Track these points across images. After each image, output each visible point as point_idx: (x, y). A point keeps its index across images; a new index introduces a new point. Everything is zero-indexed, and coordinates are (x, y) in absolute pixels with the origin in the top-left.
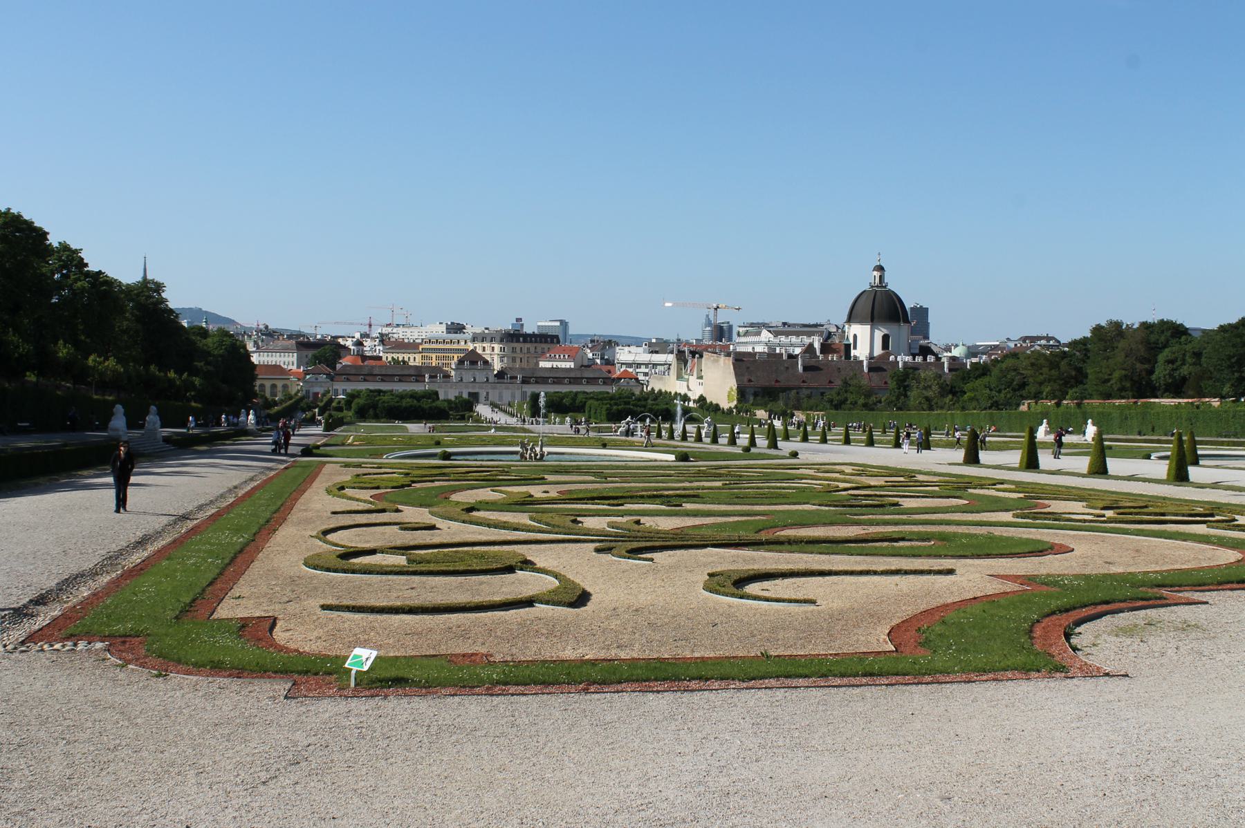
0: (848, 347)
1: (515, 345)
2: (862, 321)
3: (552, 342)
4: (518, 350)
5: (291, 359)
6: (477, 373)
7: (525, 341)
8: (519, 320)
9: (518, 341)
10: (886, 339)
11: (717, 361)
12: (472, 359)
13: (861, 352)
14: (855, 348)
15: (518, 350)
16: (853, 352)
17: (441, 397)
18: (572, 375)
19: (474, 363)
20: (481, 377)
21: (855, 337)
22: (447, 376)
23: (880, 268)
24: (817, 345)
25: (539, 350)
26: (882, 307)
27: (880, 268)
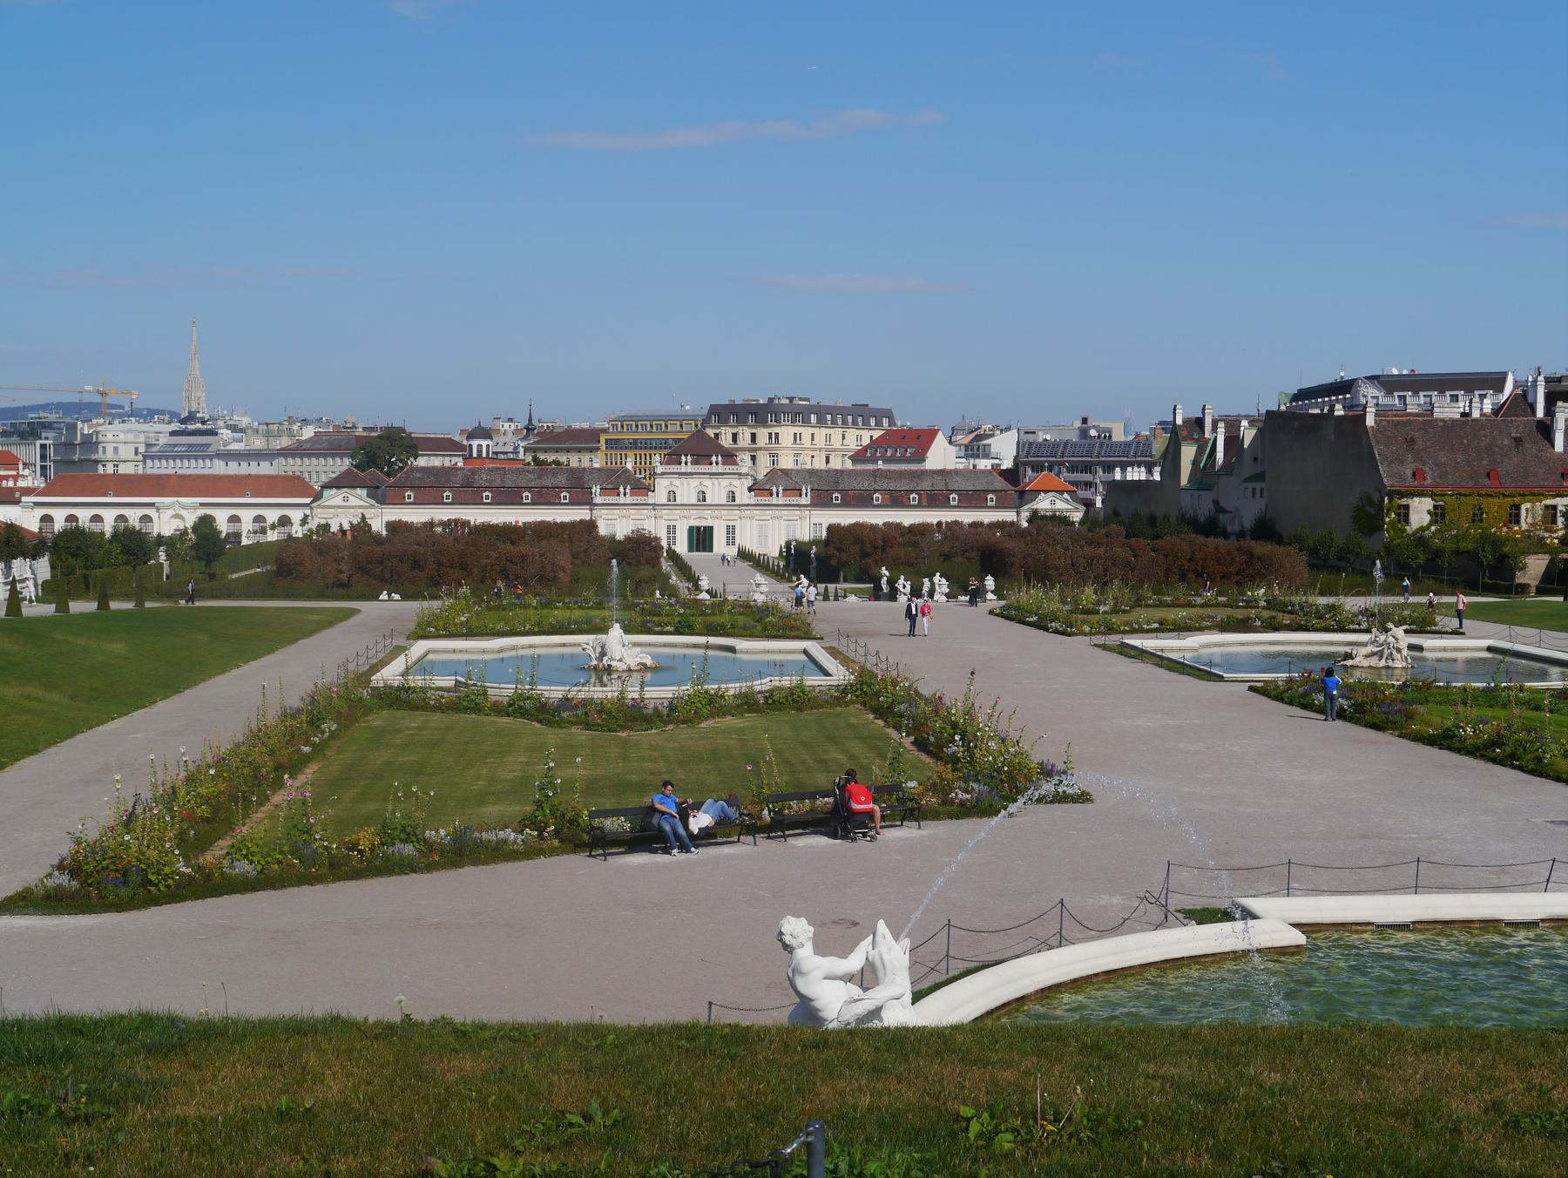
4: (806, 440)
6: (707, 482)
7: (821, 422)
9: (806, 422)
15: (806, 440)
17: (603, 530)
18: (926, 485)
19: (702, 457)
20: (717, 491)
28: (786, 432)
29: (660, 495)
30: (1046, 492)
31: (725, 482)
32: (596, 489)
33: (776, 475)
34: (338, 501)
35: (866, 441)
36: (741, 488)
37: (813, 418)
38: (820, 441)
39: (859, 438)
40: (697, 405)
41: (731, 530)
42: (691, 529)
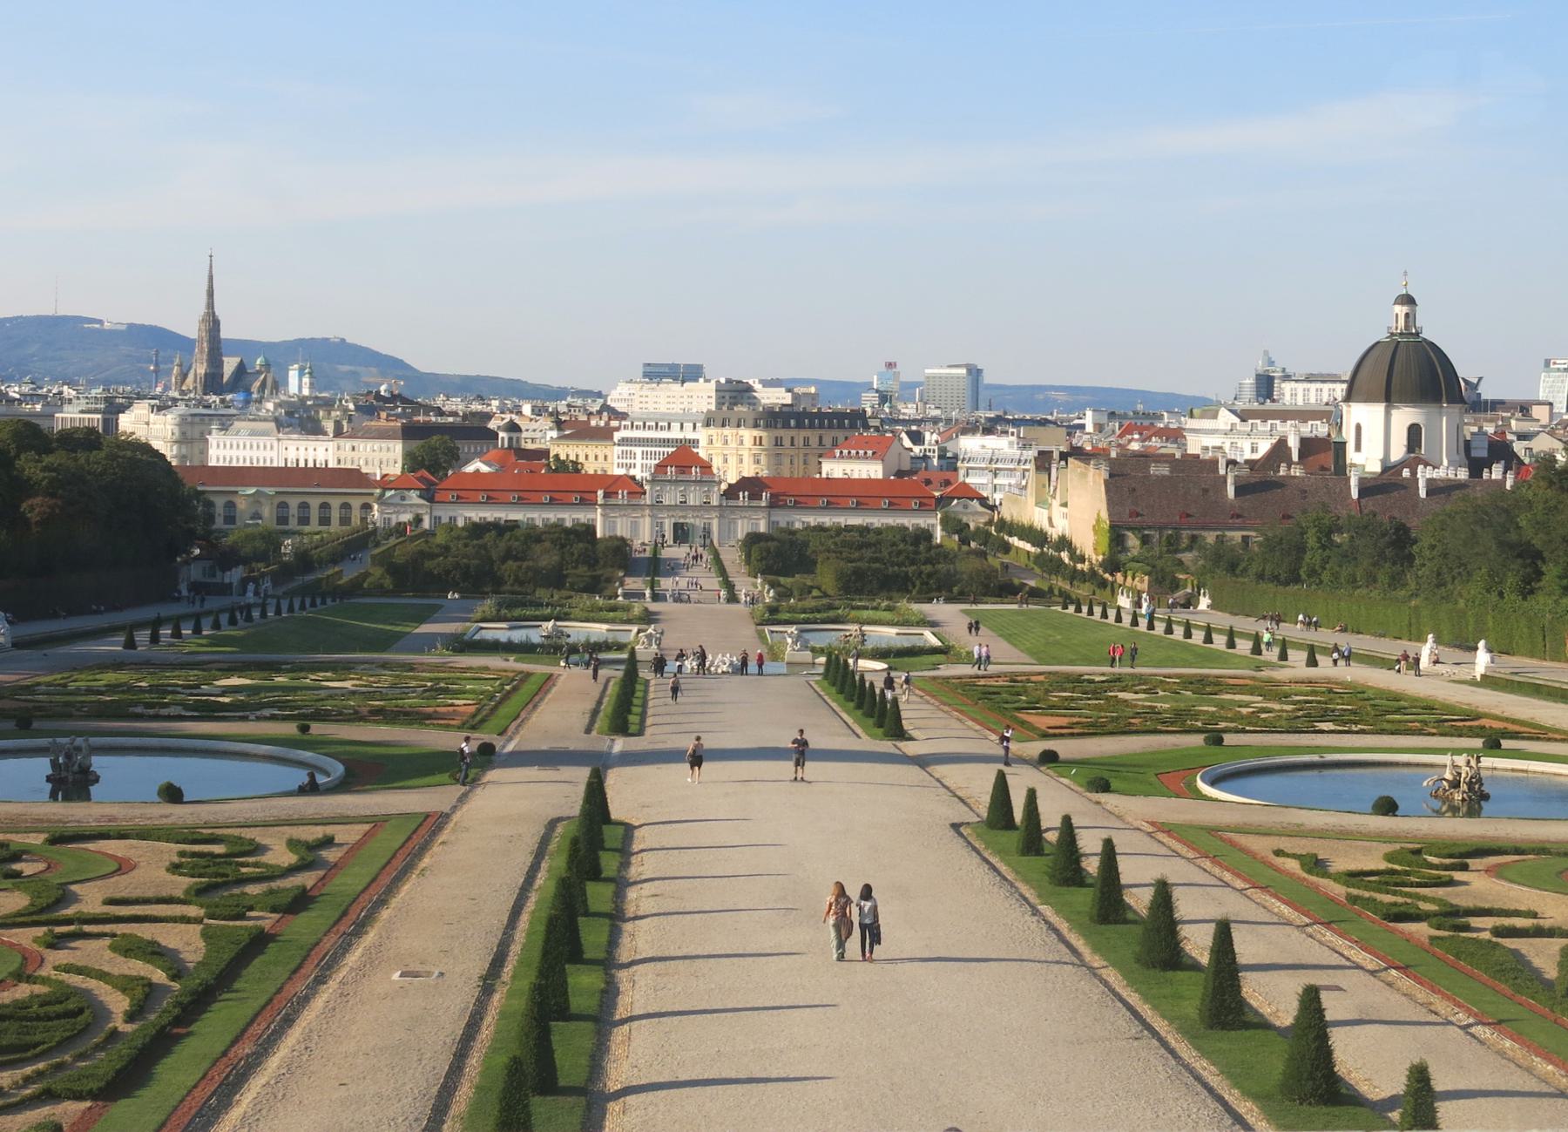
0: (1342, 446)
1: (781, 432)
2: (1369, 399)
3: (853, 426)
4: (787, 442)
5: (391, 455)
7: (799, 426)
8: (890, 365)
9: (786, 426)
10: (1414, 432)
11: (1084, 475)
12: (683, 461)
13: (1366, 459)
14: (1358, 448)
15: (787, 442)
16: (1352, 456)
19: (683, 469)
21: (1358, 428)
23: (1408, 300)
24: (1293, 443)
25: (827, 441)
26: (1412, 370)
27: (1408, 300)
32: (600, 493)
37: (792, 422)
38: (799, 442)
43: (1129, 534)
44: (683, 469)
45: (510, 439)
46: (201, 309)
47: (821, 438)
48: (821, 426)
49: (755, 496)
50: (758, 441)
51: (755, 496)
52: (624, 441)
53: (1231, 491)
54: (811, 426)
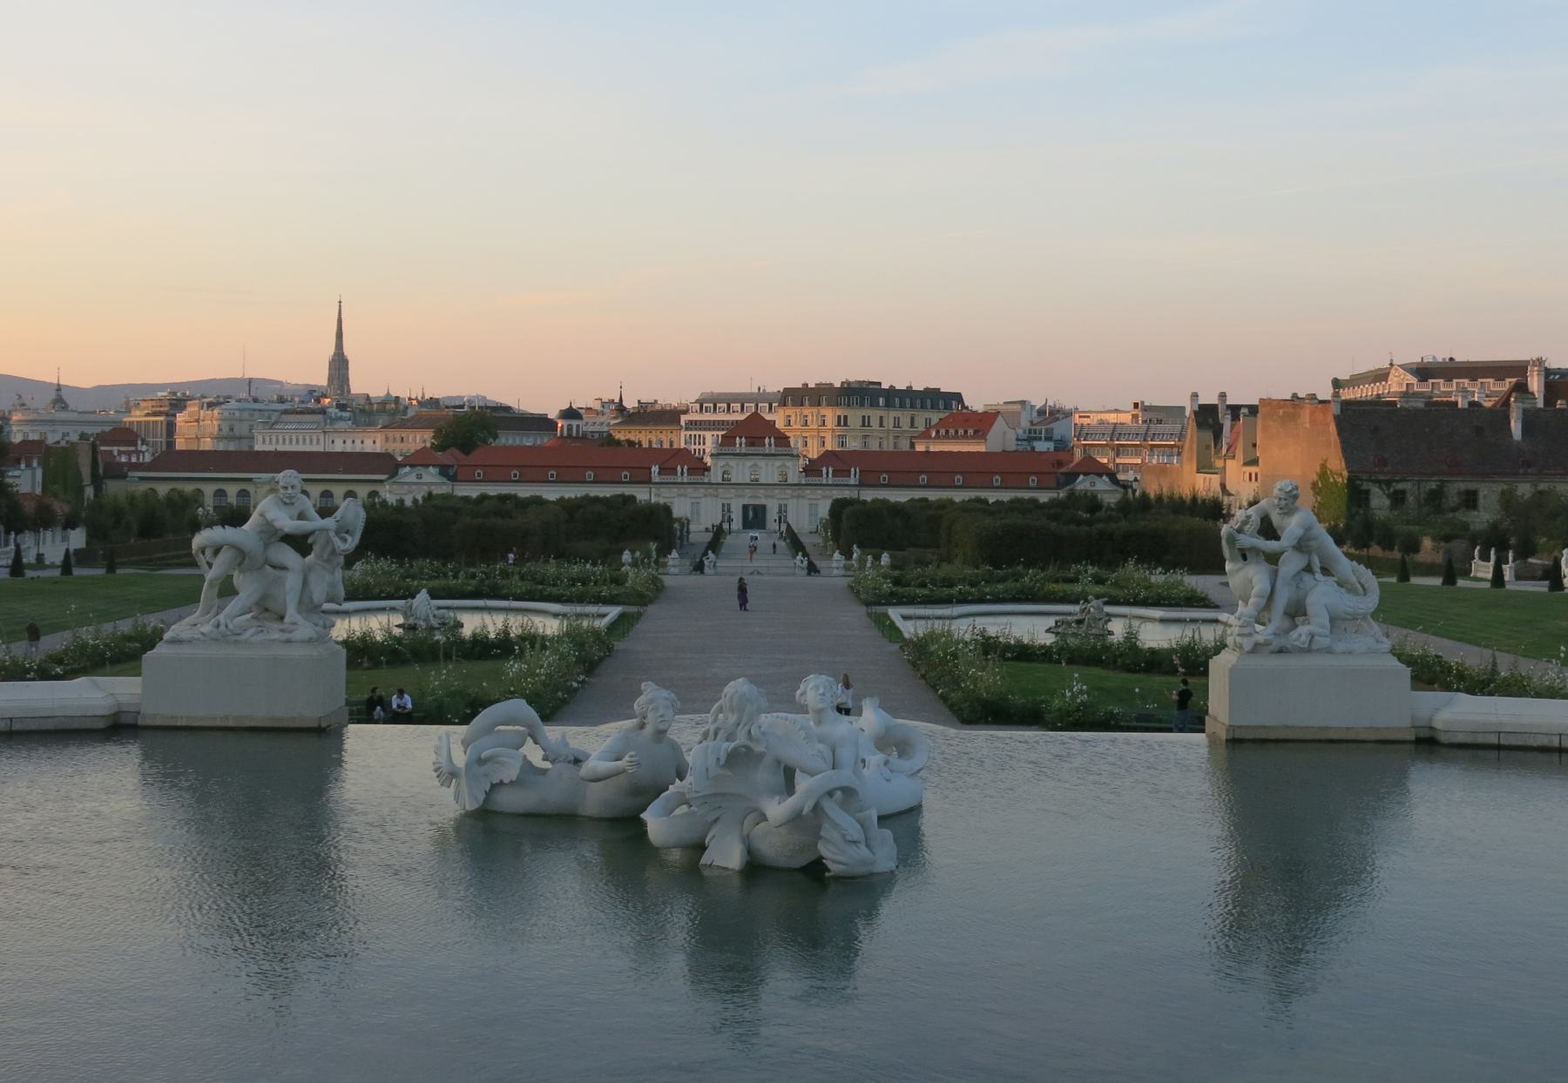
4: (875, 423)
6: (762, 463)
7: (889, 405)
9: (874, 404)
15: (875, 423)
20: (769, 471)
22: (699, 468)
28: (855, 416)
29: (715, 476)
30: (1086, 474)
31: (778, 463)
32: (655, 469)
33: (828, 457)
34: (412, 478)
35: (935, 421)
36: (794, 471)
39: (928, 421)
40: (775, 386)
41: (782, 511)
42: (745, 507)
43: (1375, 490)
44: (752, 442)
45: (570, 428)
46: (331, 350)
47: (912, 419)
48: (913, 406)
49: (841, 472)
50: (842, 421)
51: (841, 472)
52: (692, 425)
53: (1516, 428)
54: (902, 406)
